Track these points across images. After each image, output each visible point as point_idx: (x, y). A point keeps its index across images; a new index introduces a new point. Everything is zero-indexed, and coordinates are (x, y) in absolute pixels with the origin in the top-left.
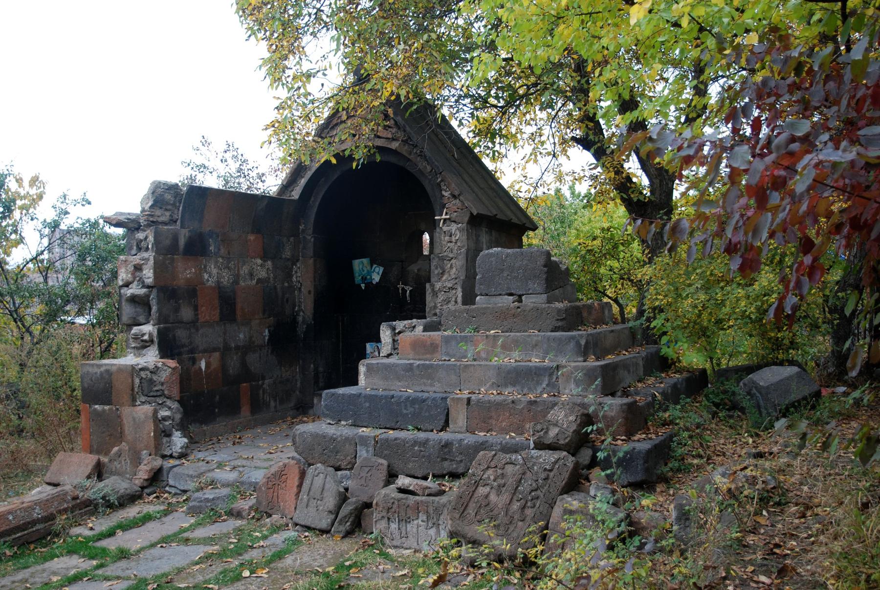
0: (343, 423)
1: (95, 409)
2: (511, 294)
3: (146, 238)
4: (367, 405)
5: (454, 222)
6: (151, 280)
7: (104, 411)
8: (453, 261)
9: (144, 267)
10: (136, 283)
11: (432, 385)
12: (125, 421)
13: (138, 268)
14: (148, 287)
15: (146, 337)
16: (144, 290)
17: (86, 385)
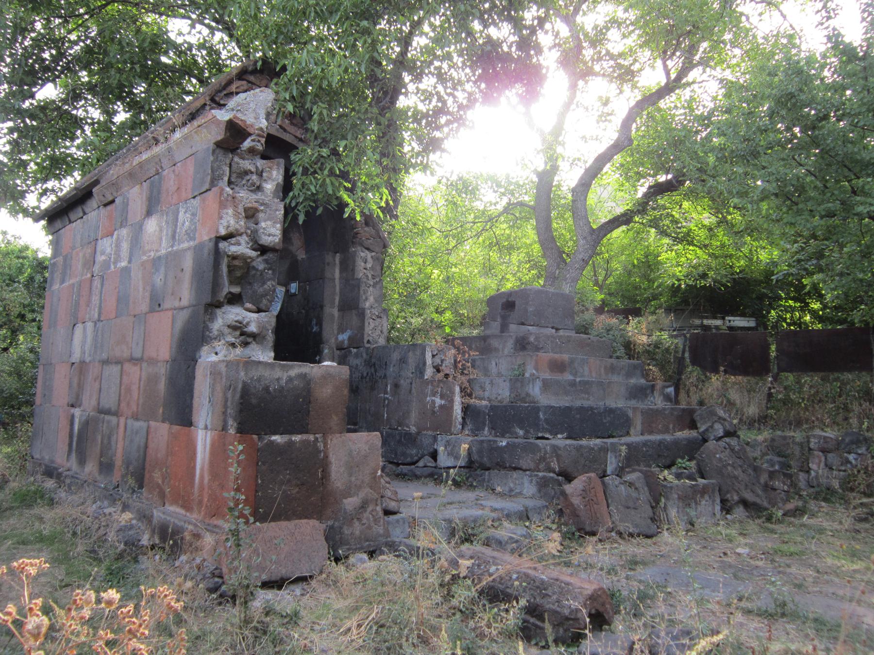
0: (559, 436)
1: (272, 442)
2: (553, 328)
3: (260, 174)
4: (578, 416)
5: (368, 249)
6: (277, 240)
7: (291, 443)
8: (371, 288)
9: (261, 215)
10: (245, 237)
11: (588, 399)
12: (332, 458)
13: (251, 214)
14: (263, 250)
15: (253, 328)
16: (254, 254)
17: (254, 401)
